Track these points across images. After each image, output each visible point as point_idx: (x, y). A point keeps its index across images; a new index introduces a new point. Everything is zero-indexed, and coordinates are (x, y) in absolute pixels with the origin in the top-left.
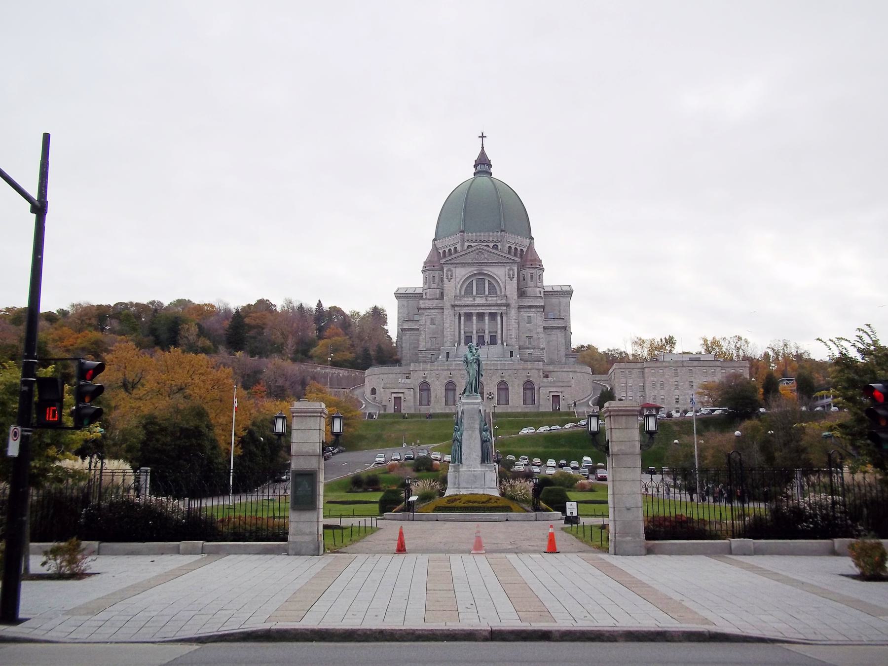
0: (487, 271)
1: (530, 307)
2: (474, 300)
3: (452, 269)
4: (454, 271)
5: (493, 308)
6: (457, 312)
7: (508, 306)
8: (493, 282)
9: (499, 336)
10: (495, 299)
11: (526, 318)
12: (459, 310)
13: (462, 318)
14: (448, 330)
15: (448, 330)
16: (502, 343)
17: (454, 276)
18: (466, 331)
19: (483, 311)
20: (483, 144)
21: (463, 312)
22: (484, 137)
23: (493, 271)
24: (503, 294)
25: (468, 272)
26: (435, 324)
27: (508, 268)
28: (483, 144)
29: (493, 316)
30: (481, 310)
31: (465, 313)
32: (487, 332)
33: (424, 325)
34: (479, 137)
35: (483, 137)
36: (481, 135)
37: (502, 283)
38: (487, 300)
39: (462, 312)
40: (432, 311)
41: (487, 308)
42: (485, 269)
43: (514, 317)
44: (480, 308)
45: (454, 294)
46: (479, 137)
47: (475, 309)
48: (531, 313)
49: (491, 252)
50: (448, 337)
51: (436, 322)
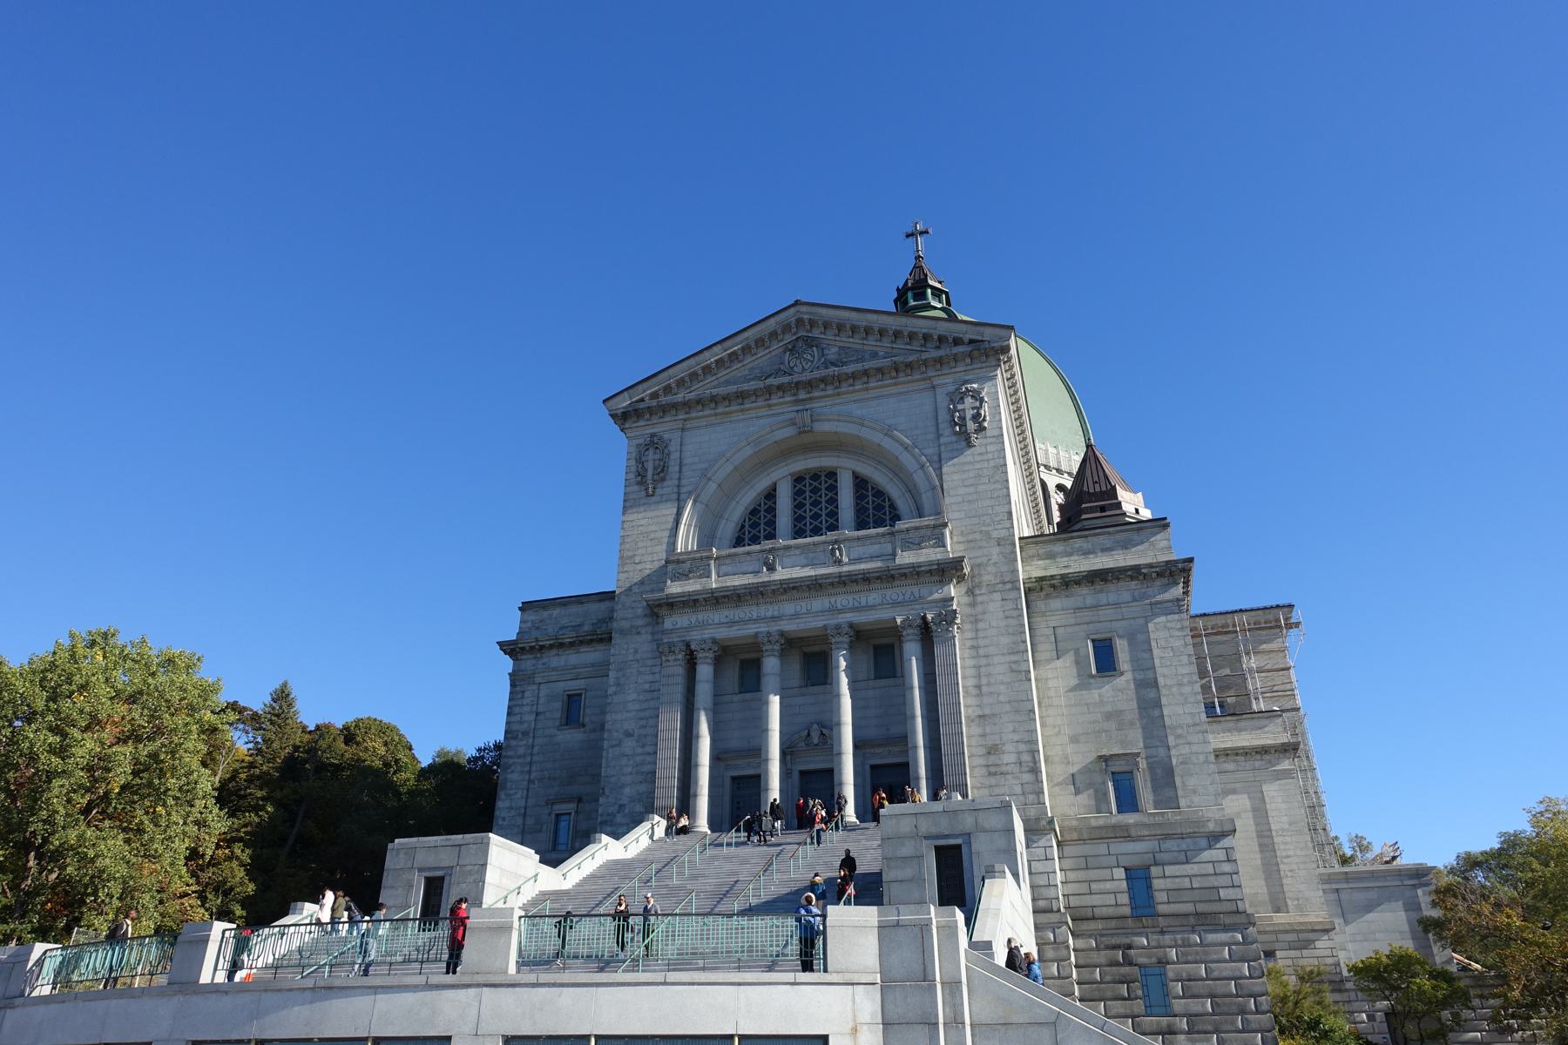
1: (1097, 578)
3: (666, 436)
4: (674, 446)
5: (873, 597)
8: (879, 477)
13: (705, 671)
14: (629, 745)
17: (673, 468)
19: (818, 623)
21: (707, 634)
26: (584, 726)
30: (804, 616)
33: (525, 734)
39: (695, 636)
40: (573, 658)
41: (842, 600)
43: (1005, 640)
44: (803, 606)
46: (908, 236)
48: (1107, 614)
49: (854, 329)
50: (623, 786)
51: (588, 715)
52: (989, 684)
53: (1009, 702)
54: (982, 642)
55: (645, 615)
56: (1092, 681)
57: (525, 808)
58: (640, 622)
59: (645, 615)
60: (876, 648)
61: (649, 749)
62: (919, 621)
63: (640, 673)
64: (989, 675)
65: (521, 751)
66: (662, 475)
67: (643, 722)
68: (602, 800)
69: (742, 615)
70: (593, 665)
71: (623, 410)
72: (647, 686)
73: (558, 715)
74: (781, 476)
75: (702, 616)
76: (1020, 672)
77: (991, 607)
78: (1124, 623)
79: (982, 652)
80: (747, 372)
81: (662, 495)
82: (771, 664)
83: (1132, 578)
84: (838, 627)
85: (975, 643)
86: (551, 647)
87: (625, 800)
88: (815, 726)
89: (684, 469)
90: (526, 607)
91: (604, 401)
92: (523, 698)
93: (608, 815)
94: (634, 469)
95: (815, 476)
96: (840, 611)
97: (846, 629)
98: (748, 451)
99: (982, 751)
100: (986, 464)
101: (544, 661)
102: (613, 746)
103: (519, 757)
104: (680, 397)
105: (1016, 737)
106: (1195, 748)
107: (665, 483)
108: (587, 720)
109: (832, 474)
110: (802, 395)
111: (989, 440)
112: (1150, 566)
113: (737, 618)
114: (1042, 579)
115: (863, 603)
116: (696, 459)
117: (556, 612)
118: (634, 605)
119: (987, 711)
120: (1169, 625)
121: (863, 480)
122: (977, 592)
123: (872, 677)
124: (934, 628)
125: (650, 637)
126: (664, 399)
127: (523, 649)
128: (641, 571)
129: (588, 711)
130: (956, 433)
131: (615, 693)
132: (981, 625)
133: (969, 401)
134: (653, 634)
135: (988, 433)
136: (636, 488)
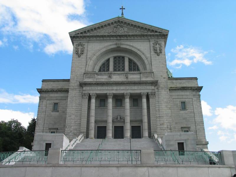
0: (127, 45)
2: (110, 77)
3: (84, 43)
5: (136, 87)
6: (86, 92)
7: (155, 83)
8: (135, 60)
9: (145, 126)
10: (138, 76)
11: (179, 104)
12: (90, 90)
13: (93, 101)
14: (73, 117)
15: (73, 117)
16: (151, 136)
17: (85, 51)
18: (98, 119)
19: (122, 92)
20: (122, 12)
21: (95, 92)
22: (124, 9)
23: (134, 46)
24: (148, 71)
25: (103, 46)
26: (58, 111)
27: (154, 42)
28: (122, 12)
29: (136, 99)
31: (96, 94)
32: (128, 119)
34: (120, 9)
35: (122, 9)
36: (121, 8)
37: (147, 59)
38: (127, 78)
39: (91, 92)
41: (128, 87)
42: (124, 43)
43: (165, 100)
44: (118, 88)
45: (83, 71)
47: (110, 88)
51: (60, 108)
52: (161, 110)
53: (166, 114)
54: (160, 100)
55: (78, 86)
56: (181, 111)
57: (43, 129)
58: (76, 87)
59: (78, 86)
60: (133, 99)
61: (78, 118)
62: (146, 94)
63: (76, 100)
64: (161, 108)
65: (42, 116)
66: (83, 52)
67: (77, 112)
68: (66, 129)
69: (103, 88)
70: (61, 97)
71: (73, 35)
72: (78, 103)
73: (52, 108)
74: (111, 56)
75: (93, 88)
76: (168, 107)
77: (162, 92)
78: (188, 99)
79: (160, 102)
80: (105, 31)
81: (82, 57)
82: (110, 101)
83: (191, 89)
84: (127, 93)
85: (158, 100)
86: (51, 91)
87: (71, 129)
88: (119, 116)
89: (88, 52)
90: (43, 81)
91: (69, 33)
92: (43, 103)
93: (68, 133)
94: (75, 50)
95: (119, 57)
96: (127, 90)
97: (129, 94)
98: (104, 50)
99: (159, 124)
100: (161, 60)
101: (48, 94)
102: (69, 117)
103: (42, 117)
104: (88, 34)
105: (167, 122)
106: (201, 127)
107: (83, 55)
108: (59, 110)
109: (123, 58)
110: (119, 38)
111: (162, 55)
112: (194, 87)
113: (102, 89)
114: (171, 87)
115: (133, 89)
116: (91, 50)
117: (52, 83)
118: (75, 83)
119: (161, 116)
120: (197, 100)
121: (131, 60)
122: (159, 88)
123: (132, 105)
124: (150, 96)
125: (79, 91)
126: (84, 35)
127: (43, 91)
128: (77, 75)
129: (60, 108)
130: (155, 52)
131: (69, 104)
132: (160, 96)
133: (158, 45)
134: (80, 90)
135: (162, 53)
136: (76, 55)
